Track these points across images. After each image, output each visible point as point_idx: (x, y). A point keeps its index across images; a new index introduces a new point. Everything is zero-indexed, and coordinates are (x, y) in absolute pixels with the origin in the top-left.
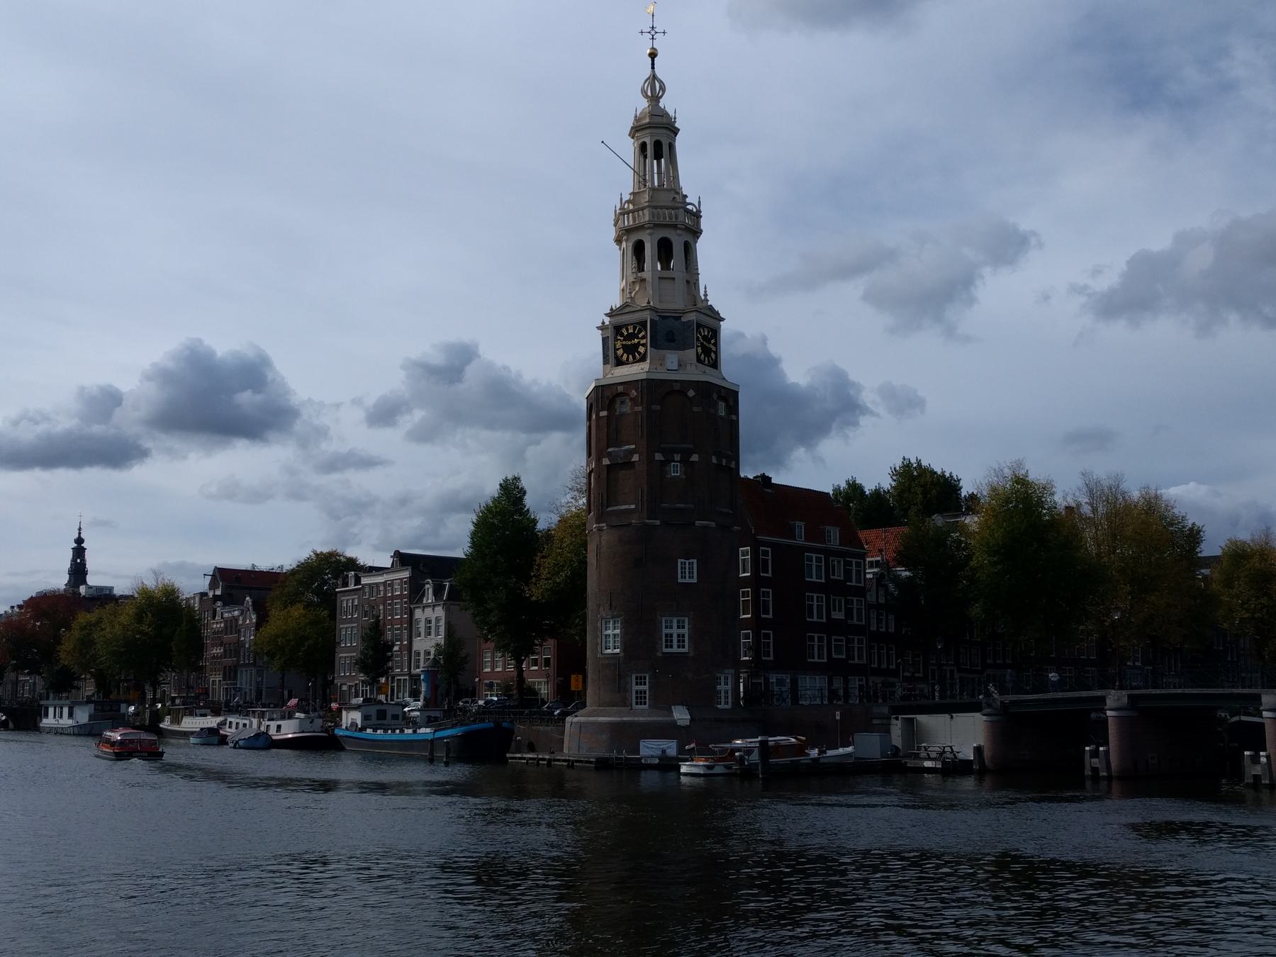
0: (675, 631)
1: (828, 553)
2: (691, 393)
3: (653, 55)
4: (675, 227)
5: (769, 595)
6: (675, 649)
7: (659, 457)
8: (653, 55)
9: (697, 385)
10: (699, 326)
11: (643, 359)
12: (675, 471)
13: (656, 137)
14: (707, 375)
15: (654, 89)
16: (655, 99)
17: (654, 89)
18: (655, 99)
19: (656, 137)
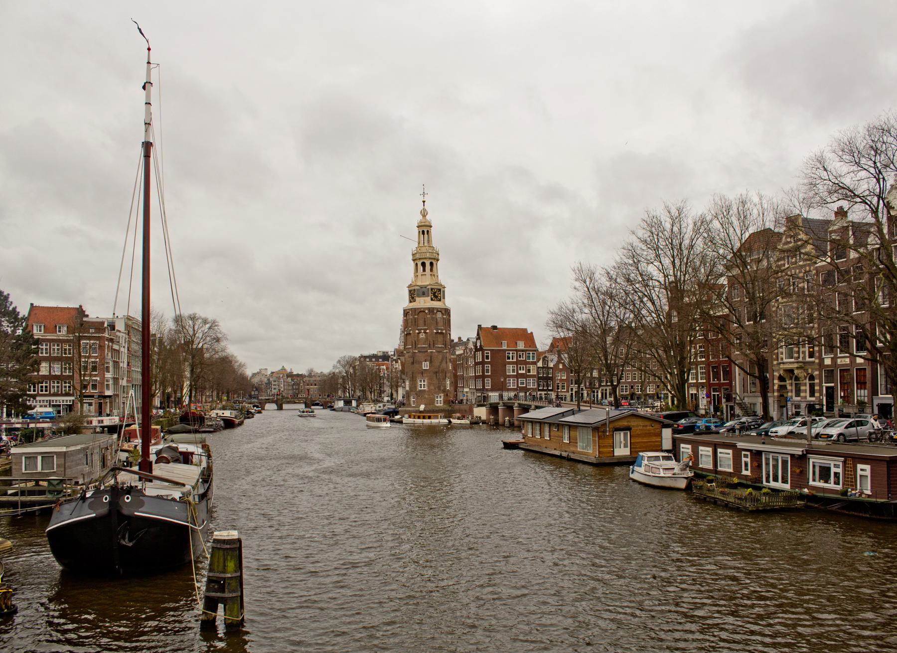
3: (424, 202)
5: (488, 367)
8: (424, 202)
9: (429, 309)
12: (422, 336)
14: (436, 304)
15: (424, 213)
16: (424, 216)
17: (424, 213)
18: (424, 216)
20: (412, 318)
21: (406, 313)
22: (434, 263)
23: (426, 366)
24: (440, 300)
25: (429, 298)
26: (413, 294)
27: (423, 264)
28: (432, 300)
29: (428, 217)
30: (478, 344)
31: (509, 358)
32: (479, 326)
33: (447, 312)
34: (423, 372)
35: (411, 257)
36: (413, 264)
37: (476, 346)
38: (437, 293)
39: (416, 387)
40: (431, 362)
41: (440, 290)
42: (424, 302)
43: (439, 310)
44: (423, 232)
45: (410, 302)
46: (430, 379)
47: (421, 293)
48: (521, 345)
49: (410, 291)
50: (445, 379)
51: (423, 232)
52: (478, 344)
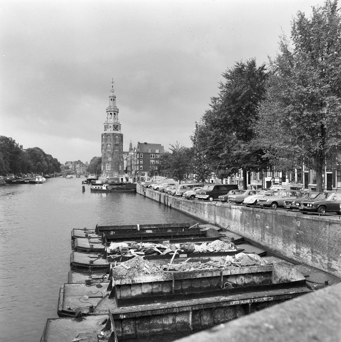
0: (108, 167)
12: (109, 146)
20: (105, 137)
22: (116, 113)
24: (118, 130)
25: (113, 129)
27: (111, 114)
31: (151, 157)
32: (139, 143)
34: (108, 162)
37: (137, 151)
38: (116, 127)
40: (112, 158)
41: (118, 126)
43: (117, 135)
44: (112, 99)
46: (112, 165)
47: (109, 127)
50: (118, 165)
51: (112, 99)
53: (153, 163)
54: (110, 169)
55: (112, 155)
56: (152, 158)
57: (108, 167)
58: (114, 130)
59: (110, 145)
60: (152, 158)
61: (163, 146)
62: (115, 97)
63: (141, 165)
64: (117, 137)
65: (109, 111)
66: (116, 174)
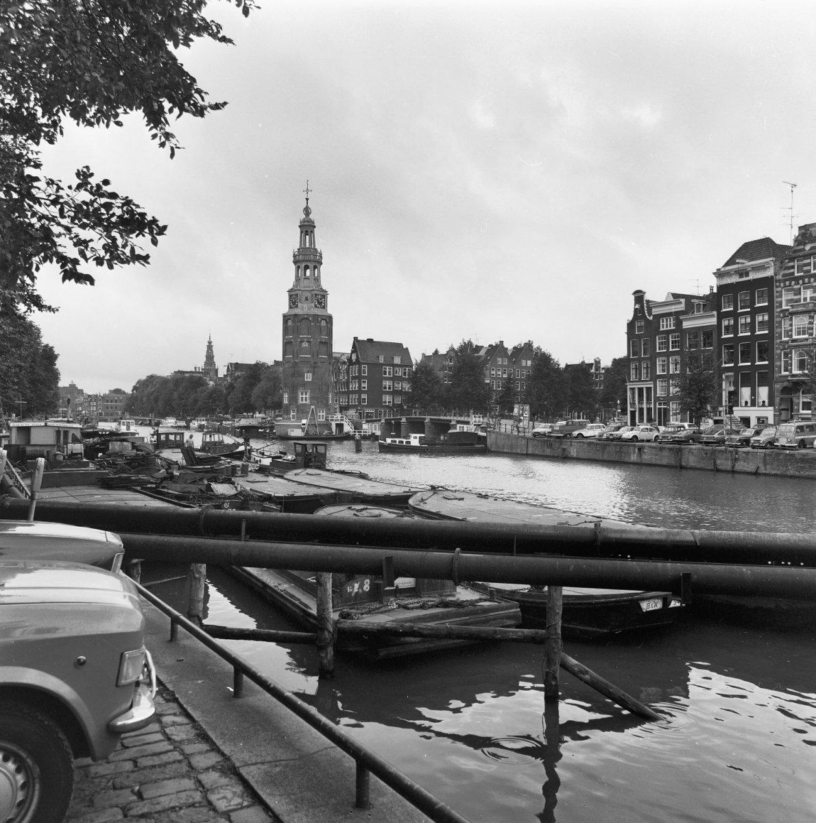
0: (304, 396)
1: (395, 366)
2: (310, 319)
3: (307, 199)
4: (309, 261)
6: (304, 402)
7: (299, 340)
8: (307, 199)
10: (316, 295)
11: (297, 307)
12: (305, 345)
13: (307, 228)
14: (318, 312)
15: (307, 211)
17: (307, 211)
19: (307, 228)
20: (292, 324)
21: (286, 318)
23: (308, 377)
24: (324, 307)
25: (313, 305)
26: (294, 298)
28: (316, 306)
29: (311, 216)
30: (354, 357)
31: (385, 373)
32: (356, 339)
33: (329, 319)
34: (304, 384)
35: (292, 259)
36: (293, 267)
38: (321, 298)
39: (297, 402)
40: (313, 375)
42: (304, 309)
44: (307, 231)
45: (290, 307)
47: (304, 298)
48: (397, 360)
49: (290, 296)
51: (307, 231)
52: (354, 357)
53: (389, 388)
54: (308, 402)
55: (314, 367)
56: (387, 375)
57: (304, 396)
58: (316, 306)
59: (309, 342)
60: (387, 375)
61: (407, 349)
62: (315, 227)
63: (364, 392)
64: (323, 323)
65: (303, 261)
66: (321, 414)
